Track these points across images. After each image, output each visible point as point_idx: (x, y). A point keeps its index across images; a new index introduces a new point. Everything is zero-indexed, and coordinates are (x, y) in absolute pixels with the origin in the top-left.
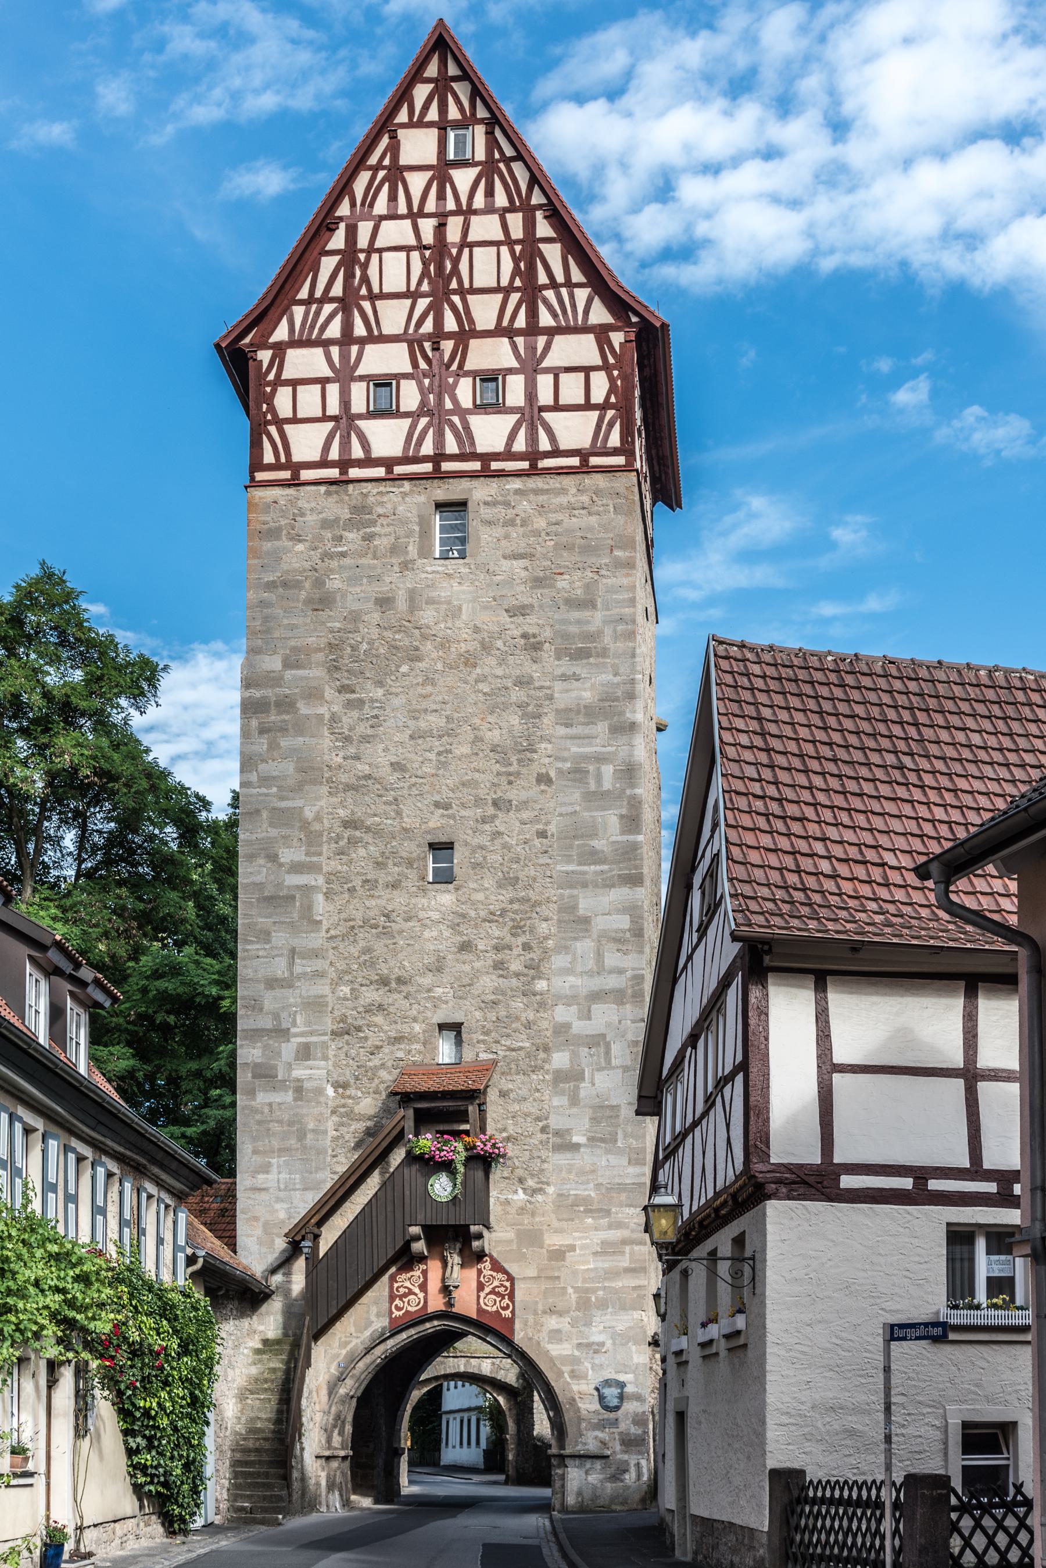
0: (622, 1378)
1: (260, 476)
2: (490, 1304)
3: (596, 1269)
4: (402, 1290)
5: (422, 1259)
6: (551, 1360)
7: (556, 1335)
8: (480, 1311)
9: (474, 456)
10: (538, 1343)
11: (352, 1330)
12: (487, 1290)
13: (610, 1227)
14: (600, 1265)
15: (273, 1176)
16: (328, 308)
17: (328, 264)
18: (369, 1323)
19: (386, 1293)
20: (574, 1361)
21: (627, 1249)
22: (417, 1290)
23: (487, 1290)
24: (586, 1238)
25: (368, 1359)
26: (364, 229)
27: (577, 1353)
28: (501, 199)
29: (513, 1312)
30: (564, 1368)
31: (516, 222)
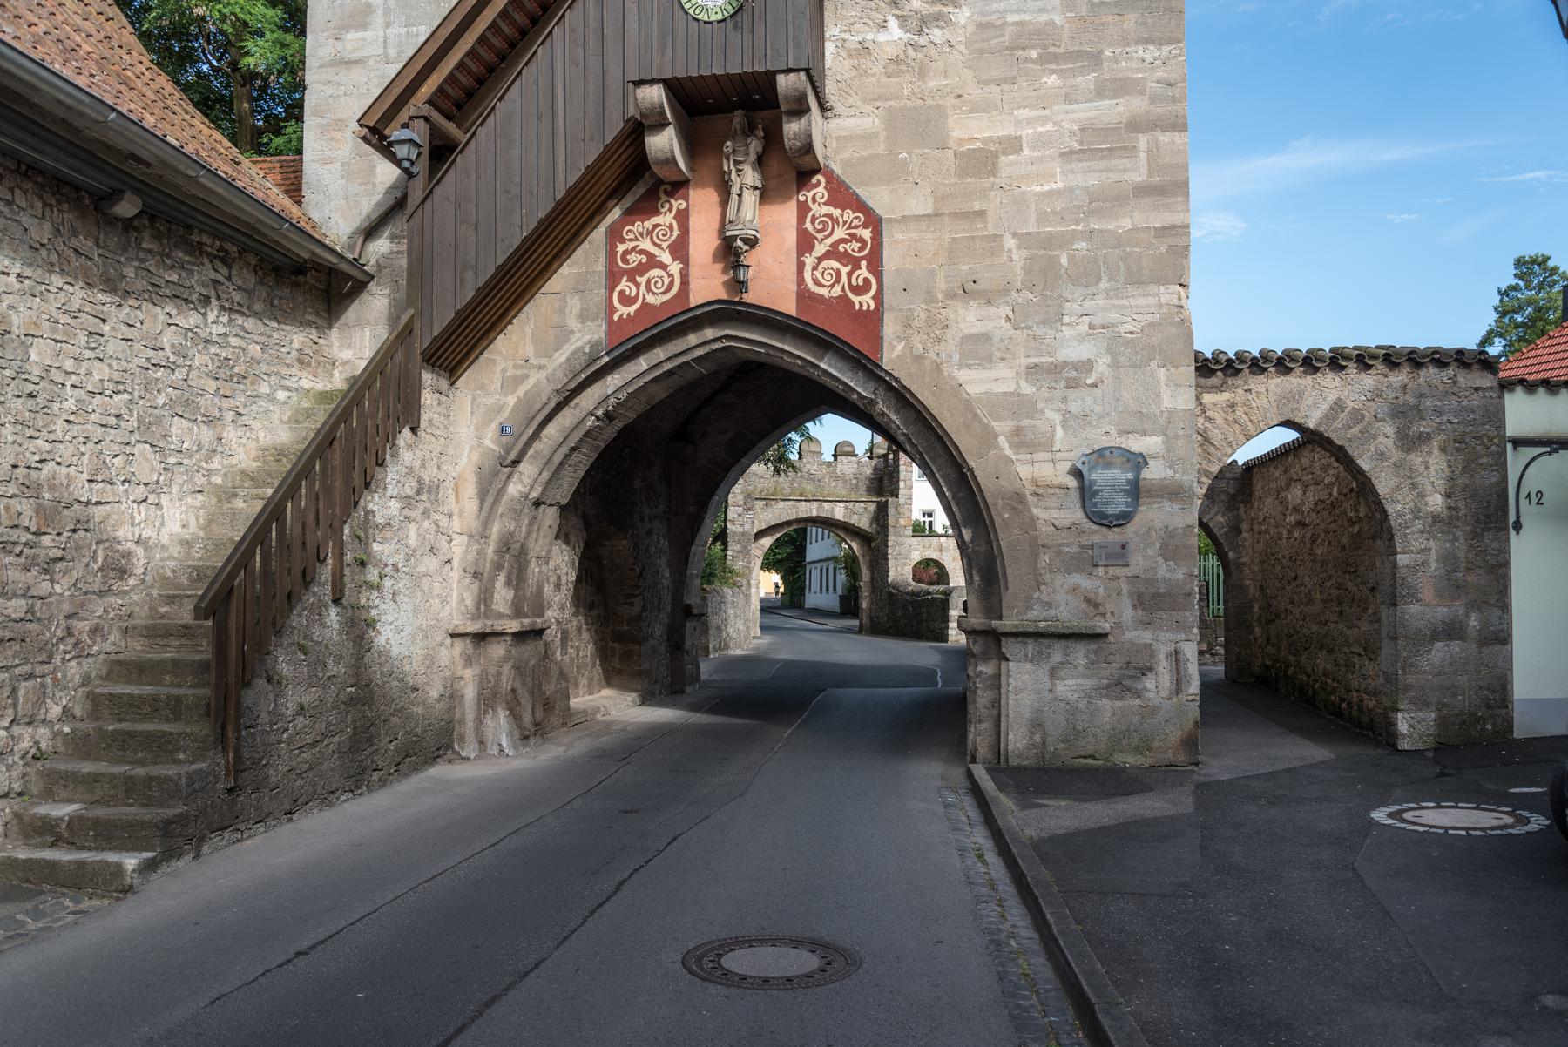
0: (1136, 444)
2: (827, 280)
3: (1069, 190)
4: (634, 259)
5: (678, 186)
6: (968, 405)
7: (979, 349)
8: (804, 296)
10: (938, 367)
11: (530, 351)
12: (820, 249)
13: (1101, 92)
14: (1078, 180)
15: (374, 34)
18: (564, 336)
19: (601, 267)
20: (1019, 406)
21: (1143, 141)
22: (665, 257)
23: (820, 249)
24: (1044, 120)
25: (566, 418)
27: (1026, 389)
29: (878, 298)
30: (998, 426)
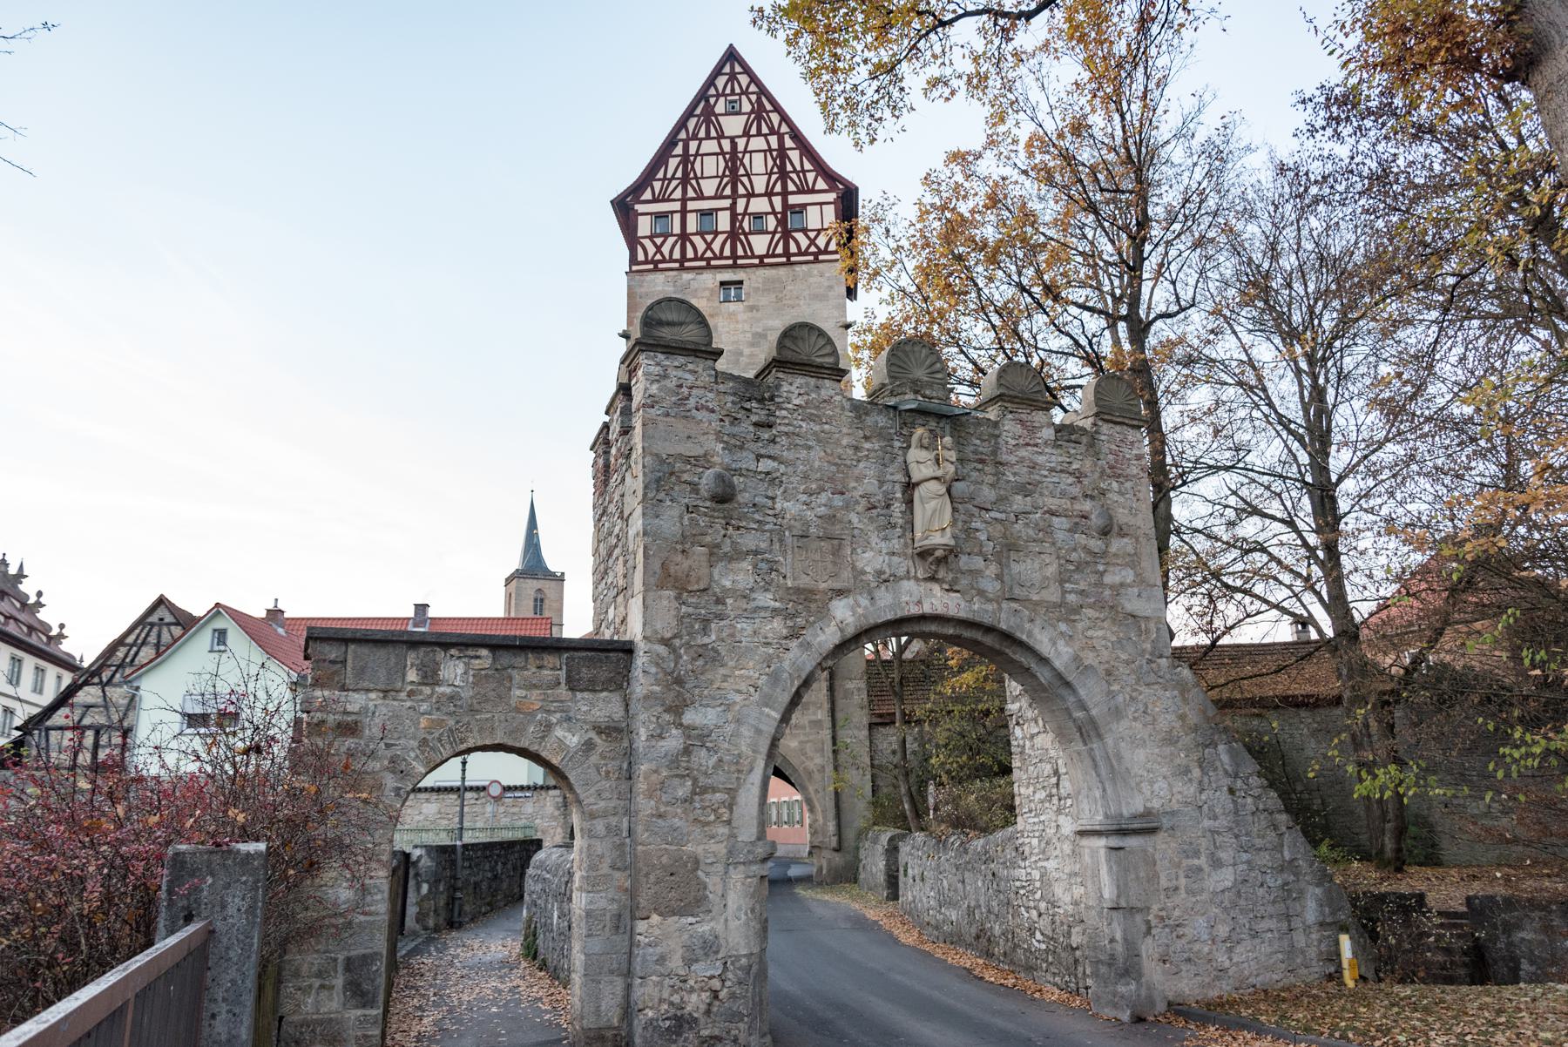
1: (635, 268)
9: (753, 256)
16: (674, 183)
17: (673, 162)
26: (693, 145)
28: (765, 130)
31: (774, 140)
